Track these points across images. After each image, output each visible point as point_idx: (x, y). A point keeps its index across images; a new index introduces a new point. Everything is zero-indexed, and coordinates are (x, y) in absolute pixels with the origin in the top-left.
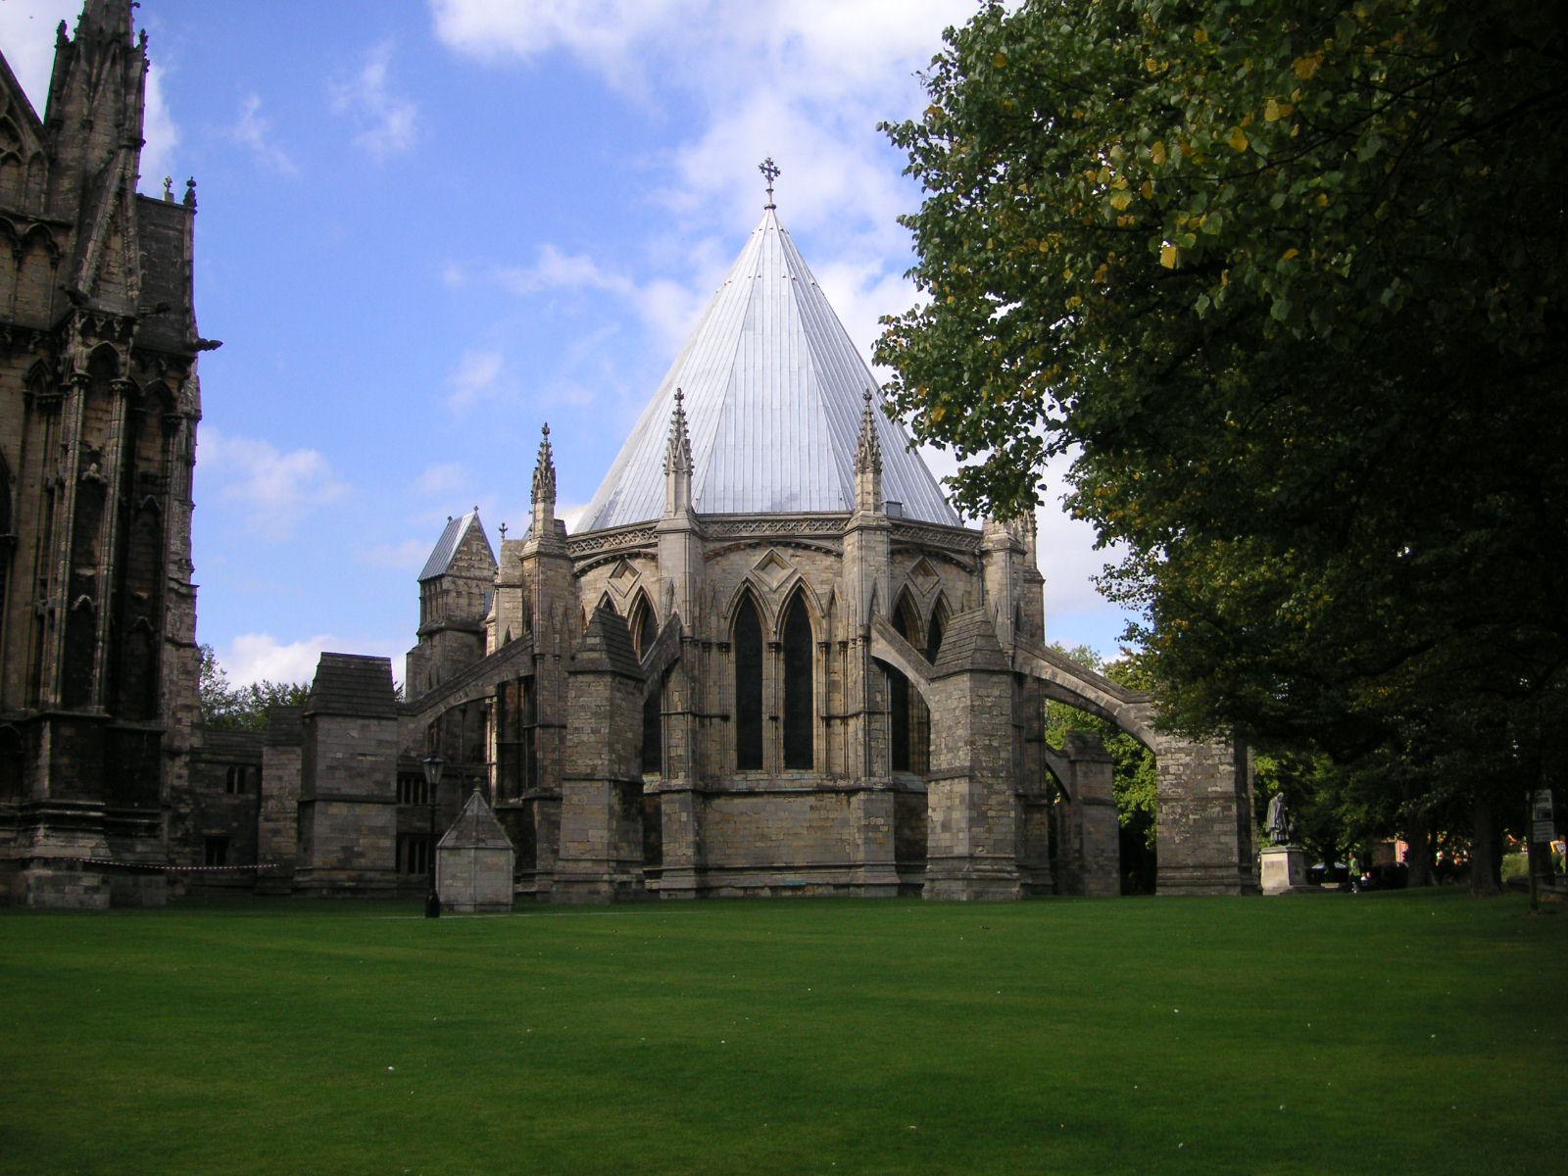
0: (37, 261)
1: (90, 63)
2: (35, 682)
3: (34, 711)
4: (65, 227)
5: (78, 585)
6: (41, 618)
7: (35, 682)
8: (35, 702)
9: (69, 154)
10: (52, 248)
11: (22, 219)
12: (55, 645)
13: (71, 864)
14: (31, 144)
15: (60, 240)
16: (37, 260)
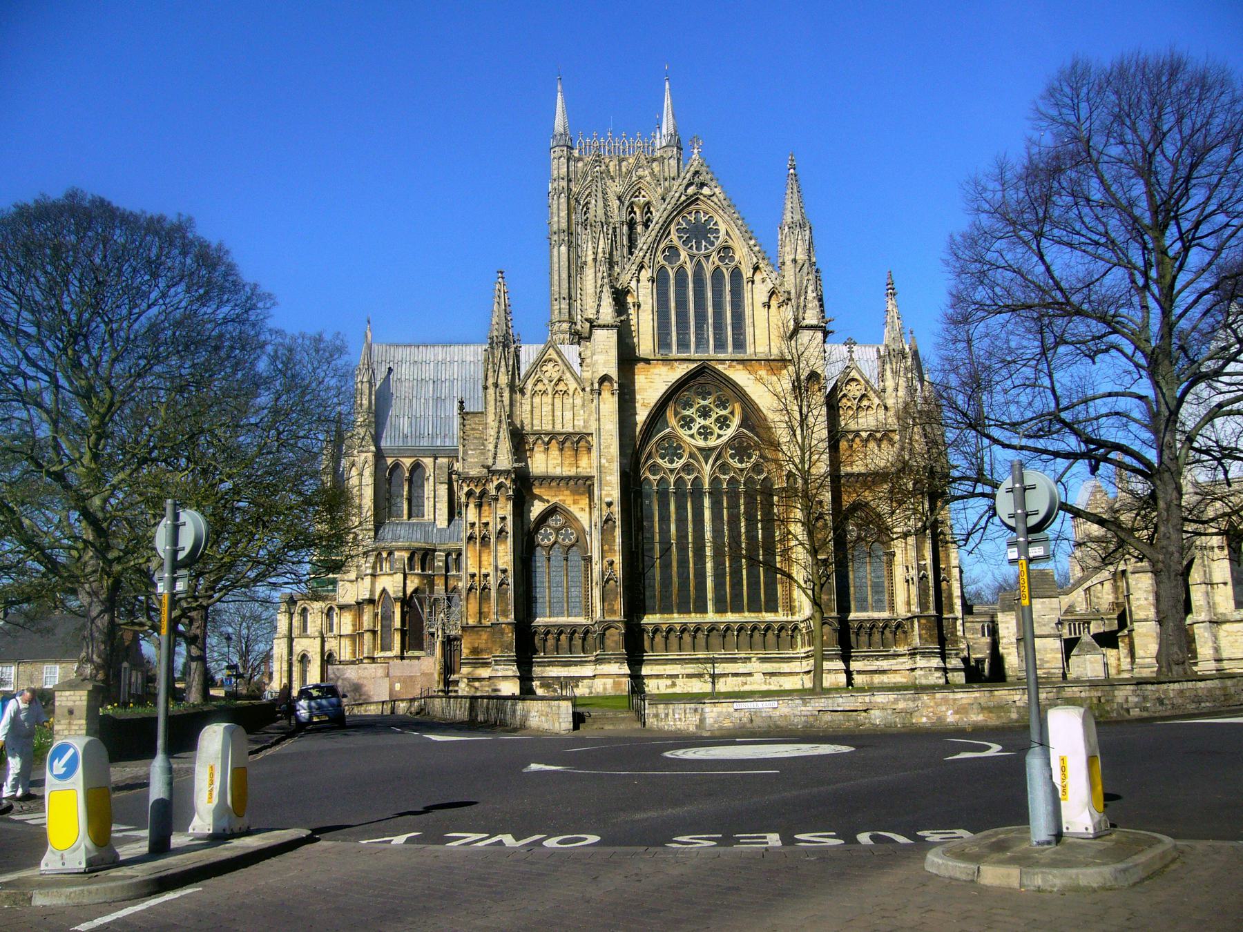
0: (884, 444)
1: (891, 363)
2: (908, 603)
3: (909, 615)
4: (894, 431)
5: (920, 568)
6: (907, 581)
7: (908, 603)
8: (909, 611)
9: (890, 402)
10: (890, 440)
11: (877, 431)
12: (914, 590)
13: (930, 669)
14: (876, 401)
15: (892, 435)
16: (884, 444)
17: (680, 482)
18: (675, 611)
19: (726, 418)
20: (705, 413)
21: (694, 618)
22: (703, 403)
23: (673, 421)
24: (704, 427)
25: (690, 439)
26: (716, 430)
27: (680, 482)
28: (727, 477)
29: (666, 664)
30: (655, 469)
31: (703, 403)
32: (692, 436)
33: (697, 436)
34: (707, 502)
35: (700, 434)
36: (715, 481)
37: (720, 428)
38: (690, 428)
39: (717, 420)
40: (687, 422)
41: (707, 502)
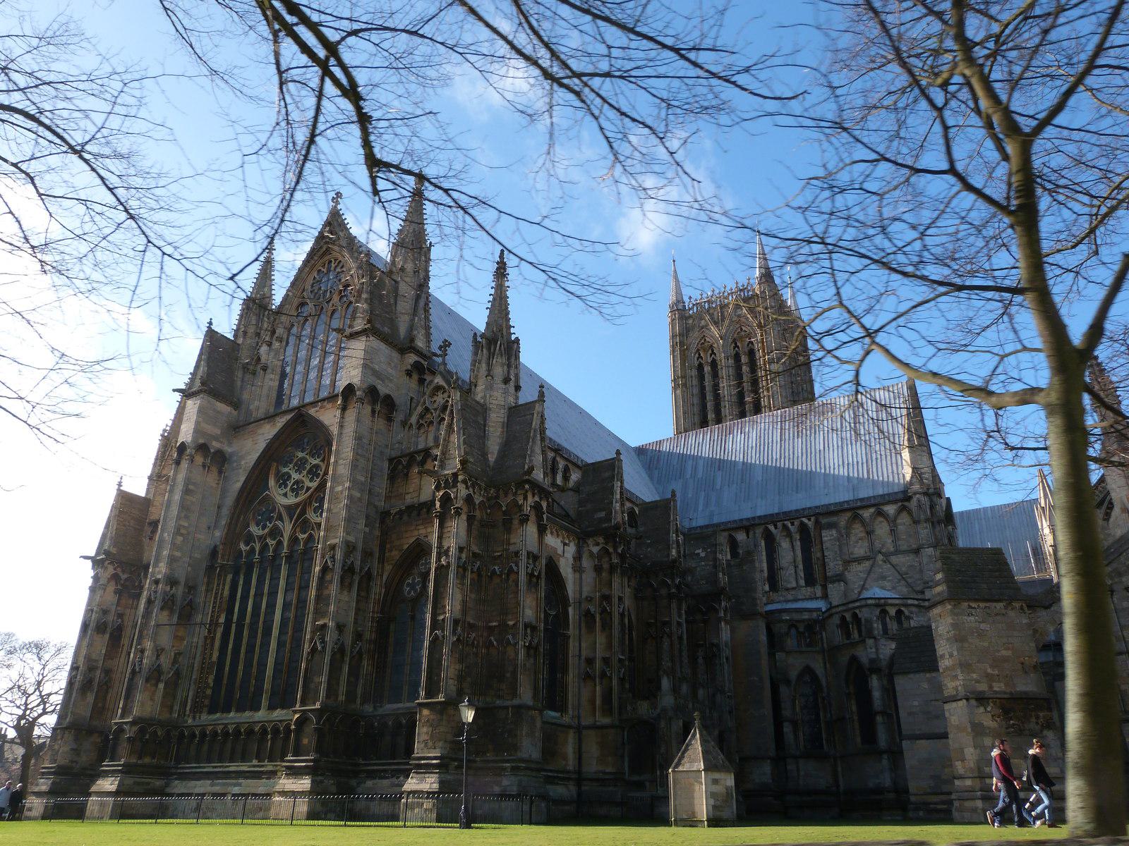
17: (265, 547)
18: (233, 709)
19: (317, 466)
20: (300, 466)
21: (247, 716)
22: (300, 455)
23: (272, 482)
24: (297, 482)
25: (283, 498)
26: (308, 483)
27: (265, 547)
28: (306, 536)
29: (199, 779)
30: (249, 539)
31: (300, 455)
32: (285, 495)
33: (290, 494)
34: (284, 572)
35: (292, 490)
36: (294, 540)
37: (311, 480)
38: (286, 486)
39: (310, 472)
40: (283, 480)
41: (284, 572)
